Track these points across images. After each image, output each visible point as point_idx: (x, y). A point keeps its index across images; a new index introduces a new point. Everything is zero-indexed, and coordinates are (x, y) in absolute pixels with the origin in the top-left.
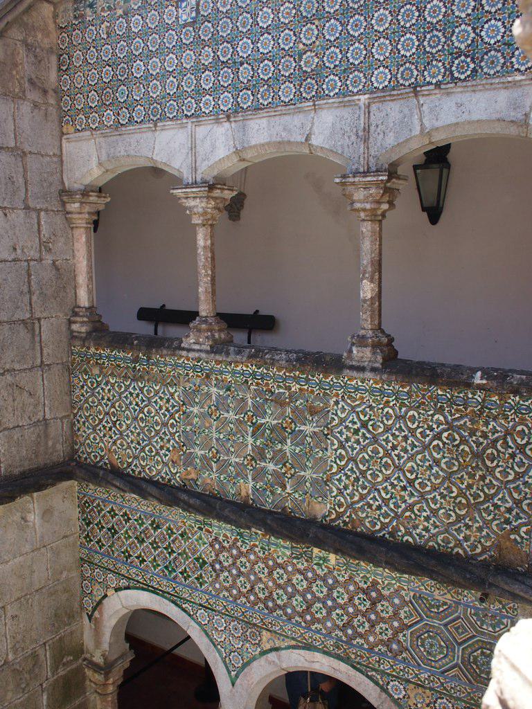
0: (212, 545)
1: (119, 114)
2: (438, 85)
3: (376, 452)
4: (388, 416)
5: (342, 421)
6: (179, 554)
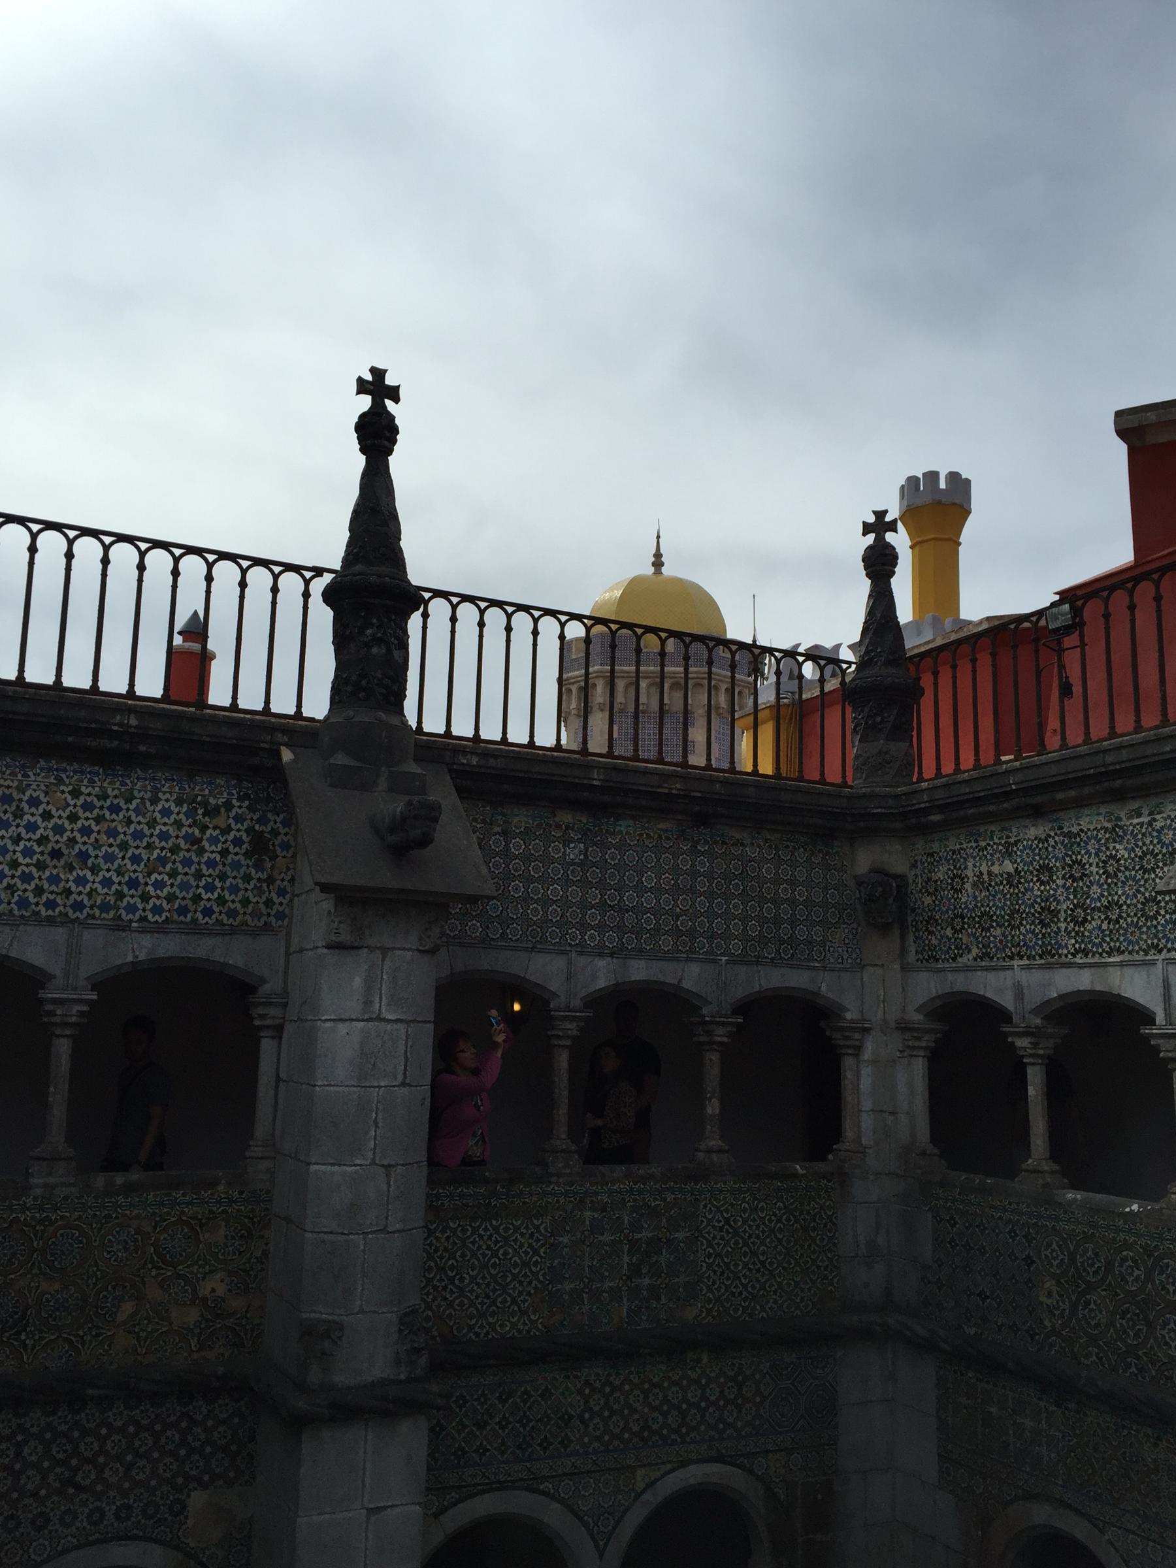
0: (580, 1392)
1: (488, 927)
2: (772, 959)
3: (736, 1243)
4: (745, 1210)
5: (710, 1221)
6: (537, 1421)
